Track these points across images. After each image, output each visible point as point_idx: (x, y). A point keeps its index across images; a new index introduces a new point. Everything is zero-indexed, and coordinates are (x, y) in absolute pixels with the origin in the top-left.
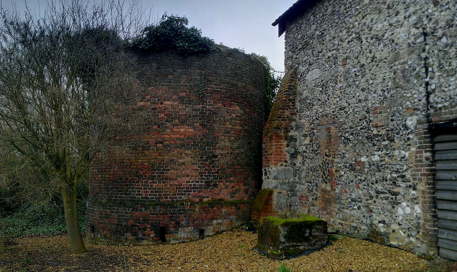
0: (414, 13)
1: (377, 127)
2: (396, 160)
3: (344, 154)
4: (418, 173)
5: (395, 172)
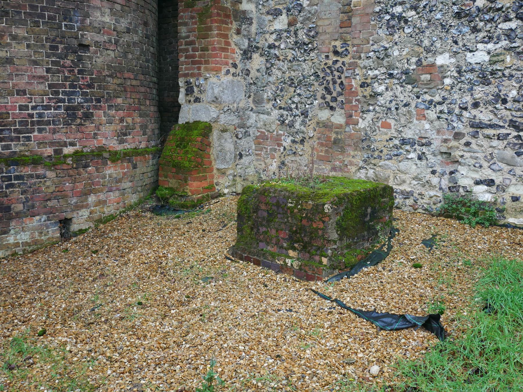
3: (386, 49)
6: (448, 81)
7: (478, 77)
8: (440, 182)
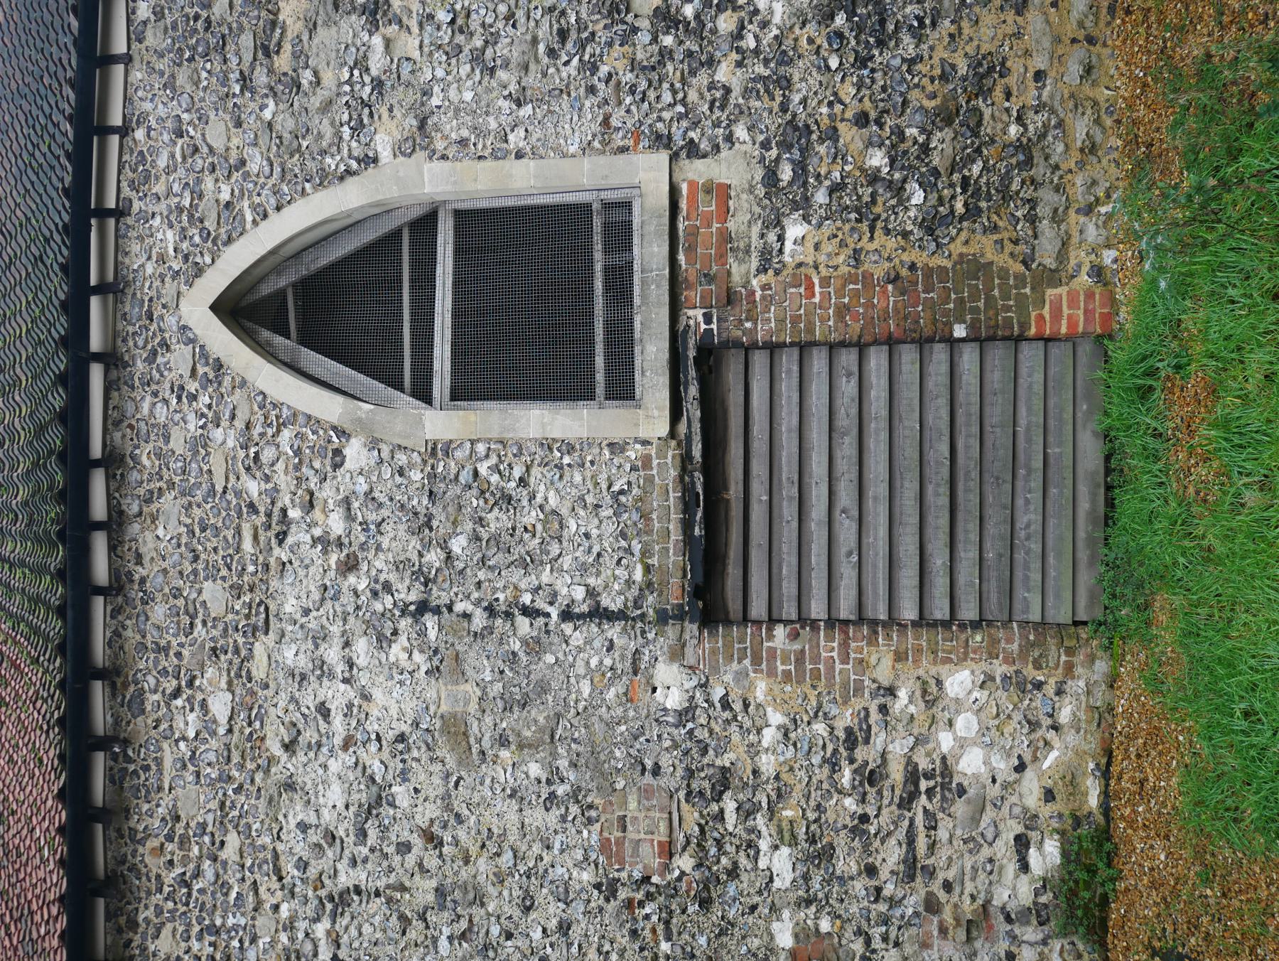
0: (347, 644)
1: (668, 851)
2: (791, 769)
5: (834, 772)
6: (825, 925)
7: (818, 866)
8: (1031, 944)
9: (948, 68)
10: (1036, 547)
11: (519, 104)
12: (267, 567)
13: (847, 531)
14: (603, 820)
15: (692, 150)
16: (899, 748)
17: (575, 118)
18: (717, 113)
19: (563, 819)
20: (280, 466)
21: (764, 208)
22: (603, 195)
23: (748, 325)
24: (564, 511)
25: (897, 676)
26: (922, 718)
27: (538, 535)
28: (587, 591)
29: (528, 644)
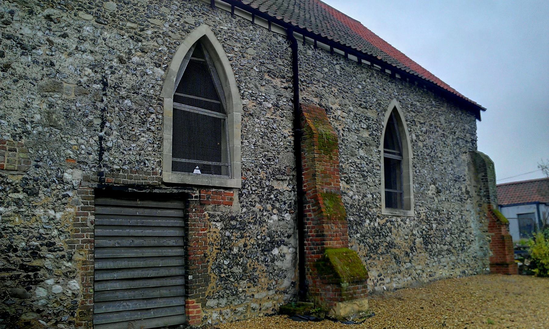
0: (92, 52)
2: (37, 221)
4: (79, 239)
5: (37, 238)
9: (256, 269)
10: (121, 309)
11: (254, 145)
12: (122, 29)
13: (126, 242)
14: (14, 142)
15: (240, 195)
16: (48, 263)
17: (250, 161)
18: (249, 203)
19: (15, 126)
20: (156, 44)
21: (225, 216)
22: (229, 167)
23: (194, 210)
24: (139, 143)
25: (76, 261)
26: (59, 272)
27: (131, 132)
28: (110, 147)
29: (91, 122)
